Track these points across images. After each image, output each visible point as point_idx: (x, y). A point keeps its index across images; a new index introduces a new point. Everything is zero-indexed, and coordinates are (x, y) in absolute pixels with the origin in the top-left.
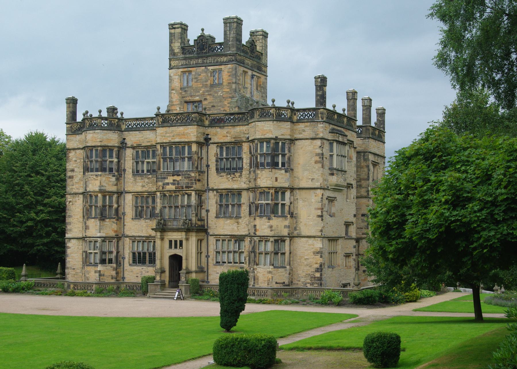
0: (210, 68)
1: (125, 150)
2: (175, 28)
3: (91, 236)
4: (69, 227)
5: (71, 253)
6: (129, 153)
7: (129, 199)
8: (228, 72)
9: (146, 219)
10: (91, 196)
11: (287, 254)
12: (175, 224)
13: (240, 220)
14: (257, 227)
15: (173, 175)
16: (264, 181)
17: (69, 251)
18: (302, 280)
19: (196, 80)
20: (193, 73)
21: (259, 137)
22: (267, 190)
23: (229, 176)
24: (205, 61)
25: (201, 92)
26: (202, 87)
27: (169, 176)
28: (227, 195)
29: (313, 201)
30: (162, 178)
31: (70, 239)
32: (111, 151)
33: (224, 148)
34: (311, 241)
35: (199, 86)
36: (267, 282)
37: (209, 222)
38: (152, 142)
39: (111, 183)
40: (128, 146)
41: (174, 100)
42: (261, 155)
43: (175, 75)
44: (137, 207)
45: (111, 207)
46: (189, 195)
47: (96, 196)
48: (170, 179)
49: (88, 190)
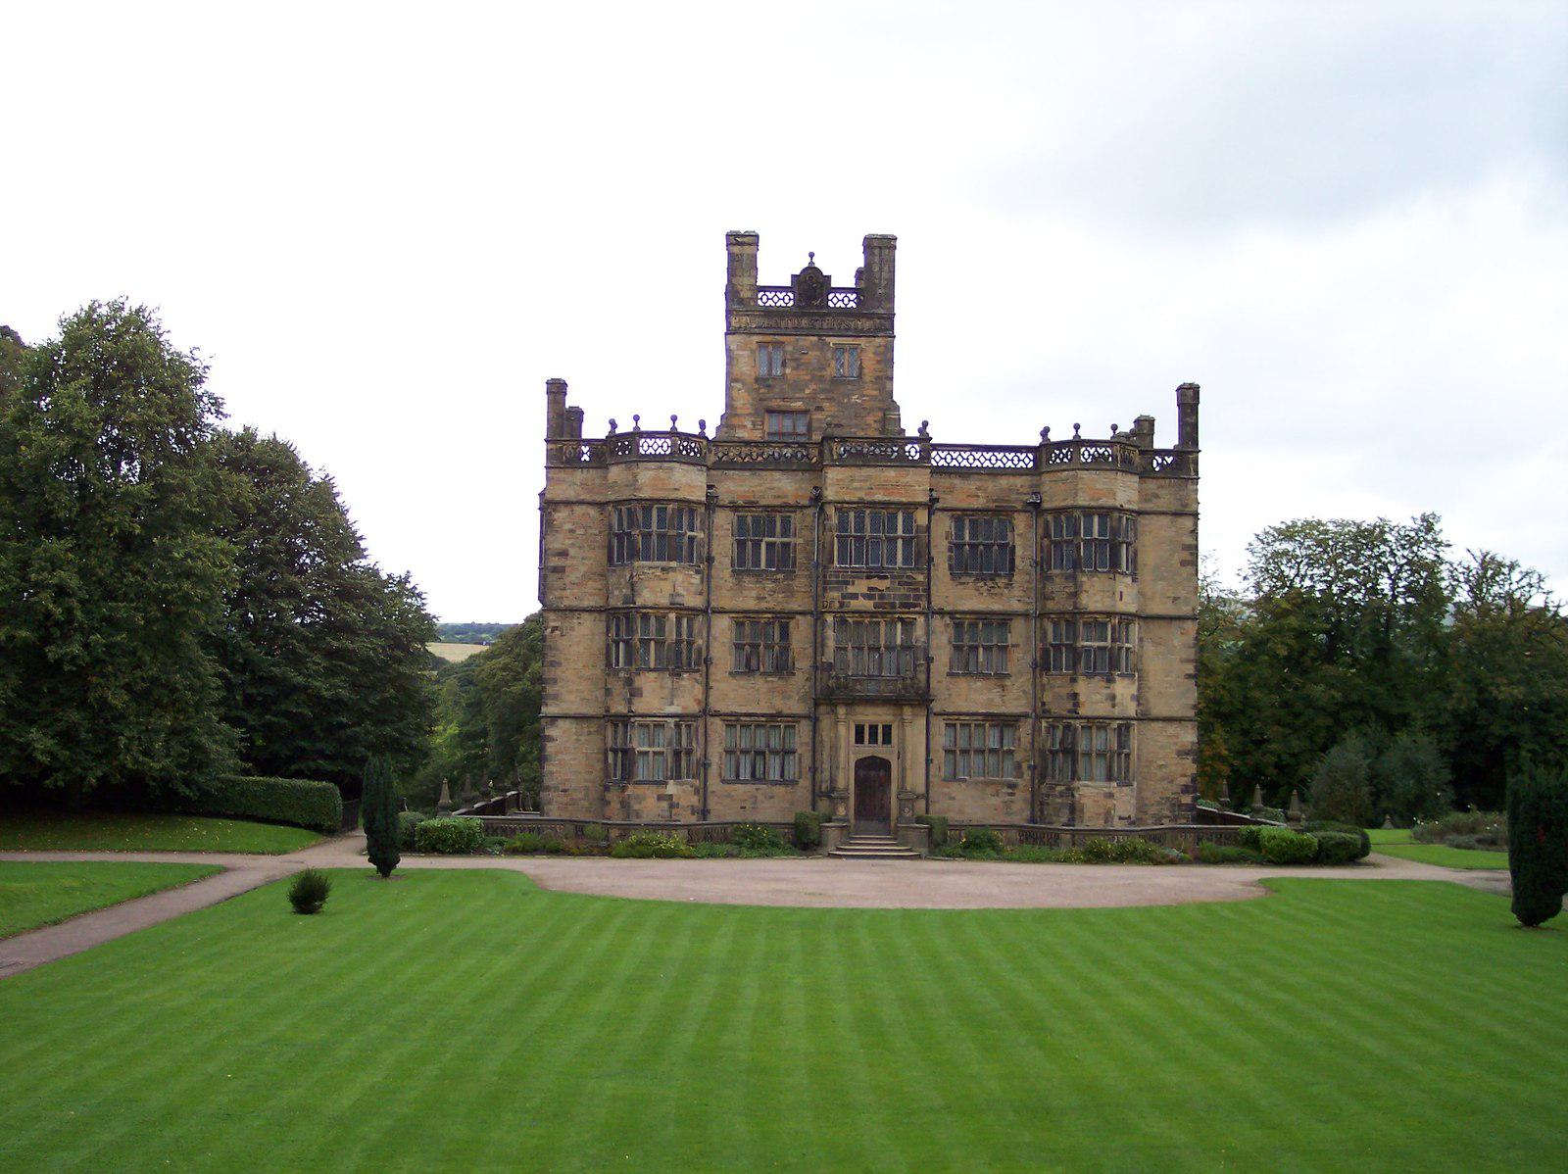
0: (832, 341)
1: (714, 512)
2: (742, 244)
3: (646, 712)
4: (550, 690)
5: (557, 753)
6: (723, 520)
7: (722, 625)
8: (875, 354)
9: (764, 674)
10: (645, 617)
11: (1134, 757)
12: (871, 689)
13: (1008, 683)
14: (1082, 698)
15: (868, 578)
16: (1098, 598)
17: (550, 747)
18: (1153, 810)
19: (794, 364)
20: (789, 348)
21: (1086, 504)
22: (1101, 619)
23: (982, 584)
24: (818, 325)
25: (807, 391)
26: (811, 381)
27: (858, 578)
28: (973, 625)
29: (1176, 643)
30: (838, 582)
31: (554, 718)
32: (692, 512)
33: (967, 522)
34: (1172, 729)
35: (802, 377)
36: (1103, 816)
37: (933, 684)
38: (785, 497)
39: (693, 589)
40: (722, 503)
41: (739, 403)
42: (1088, 543)
43: (740, 348)
44: (739, 647)
45: (690, 643)
46: (908, 625)
47: (661, 620)
48: (861, 586)
49: (638, 604)
